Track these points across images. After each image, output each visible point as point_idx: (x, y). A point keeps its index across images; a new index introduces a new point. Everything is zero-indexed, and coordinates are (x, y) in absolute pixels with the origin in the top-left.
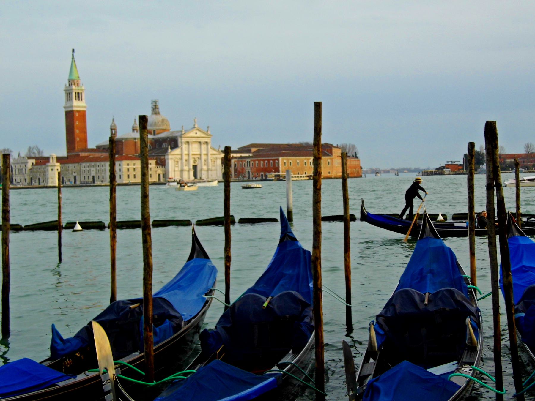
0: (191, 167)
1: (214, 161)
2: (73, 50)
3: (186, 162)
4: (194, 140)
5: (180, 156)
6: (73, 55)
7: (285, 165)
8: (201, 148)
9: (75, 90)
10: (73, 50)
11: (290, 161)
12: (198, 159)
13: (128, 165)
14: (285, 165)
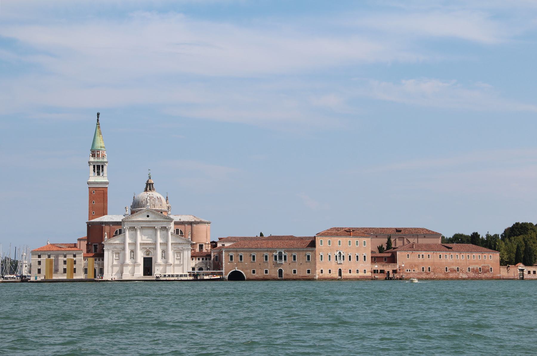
0: (141, 261)
1: (179, 252)
2: (98, 114)
3: (132, 254)
4: (144, 225)
5: (121, 246)
6: (98, 120)
7: (231, 259)
8: (156, 235)
9: (93, 162)
10: (98, 114)
11: (240, 254)
12: (152, 249)
13: (39, 257)
14: (231, 259)
